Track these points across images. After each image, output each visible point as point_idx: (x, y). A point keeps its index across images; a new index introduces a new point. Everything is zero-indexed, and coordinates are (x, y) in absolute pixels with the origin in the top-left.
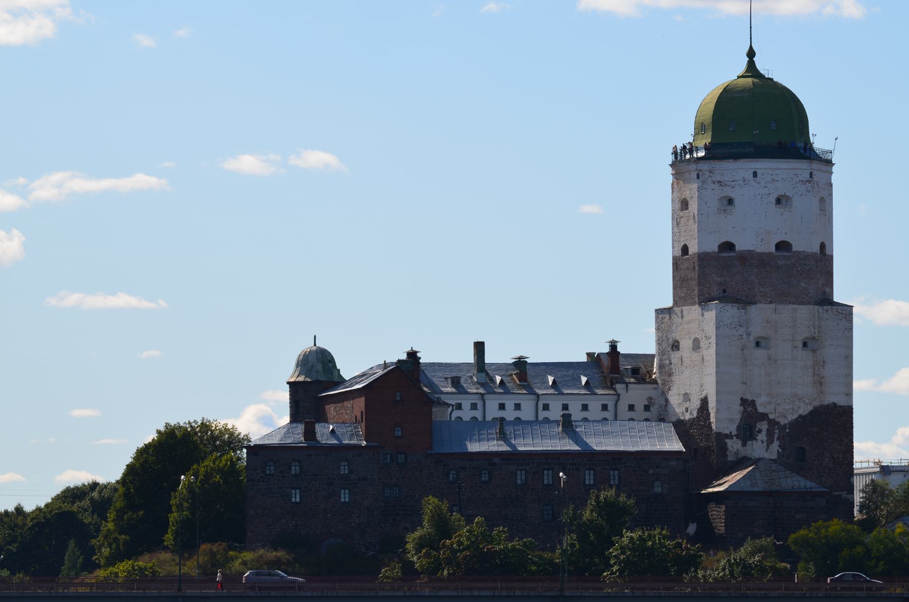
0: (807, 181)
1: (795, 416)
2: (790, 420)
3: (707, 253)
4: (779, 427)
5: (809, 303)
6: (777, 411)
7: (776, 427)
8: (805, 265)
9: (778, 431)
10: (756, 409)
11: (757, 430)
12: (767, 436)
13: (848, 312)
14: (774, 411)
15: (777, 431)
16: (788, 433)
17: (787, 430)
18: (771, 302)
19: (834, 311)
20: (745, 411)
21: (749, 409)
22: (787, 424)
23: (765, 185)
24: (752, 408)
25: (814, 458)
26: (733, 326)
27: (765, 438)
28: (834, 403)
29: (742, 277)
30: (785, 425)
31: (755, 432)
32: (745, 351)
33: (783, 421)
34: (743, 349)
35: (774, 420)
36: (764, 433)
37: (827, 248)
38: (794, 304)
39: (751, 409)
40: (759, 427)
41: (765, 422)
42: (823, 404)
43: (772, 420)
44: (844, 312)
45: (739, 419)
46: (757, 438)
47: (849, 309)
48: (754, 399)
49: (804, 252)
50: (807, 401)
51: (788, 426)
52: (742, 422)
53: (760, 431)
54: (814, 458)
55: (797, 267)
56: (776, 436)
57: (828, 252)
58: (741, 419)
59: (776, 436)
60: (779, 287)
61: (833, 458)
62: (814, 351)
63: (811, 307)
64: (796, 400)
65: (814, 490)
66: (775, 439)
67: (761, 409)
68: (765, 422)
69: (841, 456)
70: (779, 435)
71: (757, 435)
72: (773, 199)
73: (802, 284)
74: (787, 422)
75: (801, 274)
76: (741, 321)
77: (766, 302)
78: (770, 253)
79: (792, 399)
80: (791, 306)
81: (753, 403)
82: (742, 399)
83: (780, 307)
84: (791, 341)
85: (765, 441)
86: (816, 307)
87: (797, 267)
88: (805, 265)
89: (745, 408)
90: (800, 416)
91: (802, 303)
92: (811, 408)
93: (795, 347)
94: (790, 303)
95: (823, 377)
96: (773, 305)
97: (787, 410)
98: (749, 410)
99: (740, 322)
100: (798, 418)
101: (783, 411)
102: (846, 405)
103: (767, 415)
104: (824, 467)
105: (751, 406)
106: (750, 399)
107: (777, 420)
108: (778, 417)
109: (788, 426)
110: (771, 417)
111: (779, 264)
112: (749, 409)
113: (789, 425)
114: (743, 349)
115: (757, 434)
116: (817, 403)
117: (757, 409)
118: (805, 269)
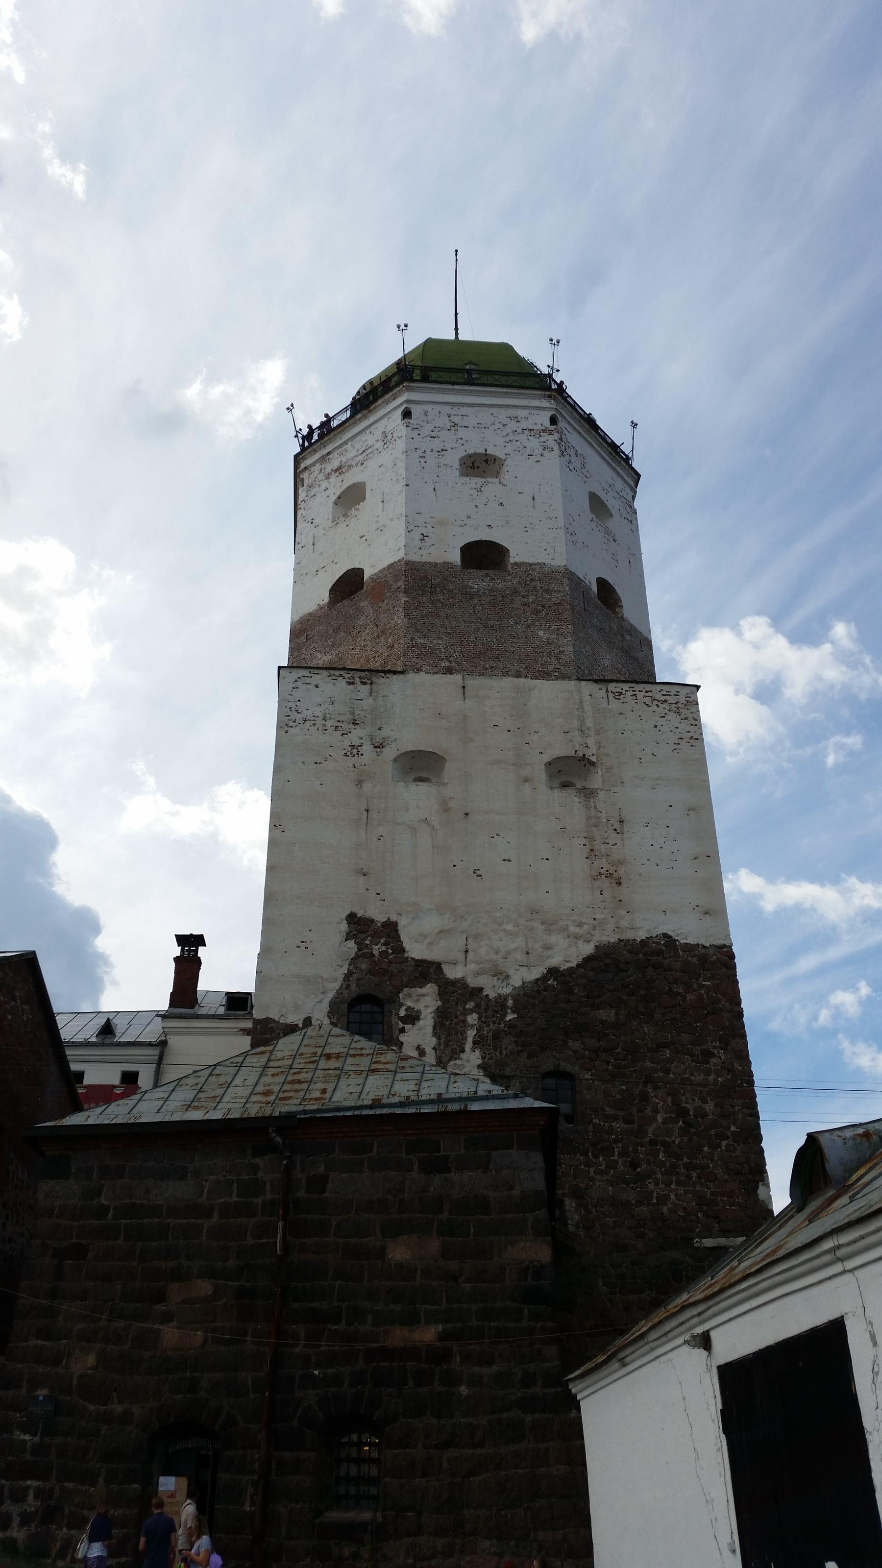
0: (544, 431)
1: (536, 974)
2: (518, 984)
3: (310, 614)
4: (478, 1006)
5: (563, 677)
6: (470, 955)
7: (470, 1005)
8: (547, 591)
9: (475, 1016)
10: (400, 949)
11: (402, 1013)
12: (435, 1034)
13: (682, 699)
14: (461, 956)
15: (472, 1019)
16: (511, 1025)
17: (510, 1017)
18: (449, 671)
19: (640, 695)
20: (363, 954)
21: (376, 949)
22: (509, 995)
23: (433, 434)
24: (385, 944)
25: (609, 1111)
26: (329, 723)
27: (429, 1041)
28: (665, 935)
29: (376, 628)
30: (501, 1001)
31: (394, 1020)
32: (367, 787)
33: (492, 988)
34: (359, 783)
35: (460, 983)
36: (427, 1022)
37: (624, 603)
38: (518, 676)
39: (384, 948)
40: (409, 1003)
41: (431, 989)
42: (629, 935)
43: (454, 983)
44: (670, 699)
45: (341, 978)
46: (403, 1038)
47: (684, 691)
48: (394, 918)
49: (542, 565)
50: (573, 929)
51: (510, 1002)
52: (348, 987)
53: (413, 1017)
54: (609, 1111)
55: (523, 596)
56: (471, 1034)
57: (628, 612)
58: (347, 977)
59: (471, 1034)
60: (472, 639)
61: (682, 1113)
62: (588, 794)
63: (571, 685)
64: (537, 924)
65: (475, 1107)
66: (469, 1045)
67: (416, 950)
68: (431, 989)
69: (710, 1107)
70: (478, 1030)
71: (402, 1030)
72: (454, 458)
73: (541, 633)
74: (508, 990)
75: (536, 612)
76: (357, 712)
77: (436, 670)
78: (447, 566)
79: (522, 921)
80: (508, 682)
81: (390, 930)
82: (352, 918)
83: (474, 683)
84: (514, 764)
85: (429, 1050)
86: (587, 688)
87: (523, 596)
88: (547, 591)
89: (360, 946)
90: (553, 972)
91: (544, 675)
92: (588, 949)
93: (526, 780)
94: (506, 673)
95: (621, 862)
96: (457, 678)
97: (508, 953)
98: (376, 953)
99: (353, 713)
100: (544, 979)
101: (494, 957)
102: (707, 945)
103: (437, 966)
104: (653, 1142)
105: (383, 940)
106: (380, 918)
107: (473, 982)
108: (477, 974)
109: (510, 1002)
110: (452, 973)
111: (471, 588)
112: (376, 949)
113: (515, 1000)
114: (359, 783)
115: (401, 1025)
116: (609, 937)
117: (403, 950)
118: (549, 600)
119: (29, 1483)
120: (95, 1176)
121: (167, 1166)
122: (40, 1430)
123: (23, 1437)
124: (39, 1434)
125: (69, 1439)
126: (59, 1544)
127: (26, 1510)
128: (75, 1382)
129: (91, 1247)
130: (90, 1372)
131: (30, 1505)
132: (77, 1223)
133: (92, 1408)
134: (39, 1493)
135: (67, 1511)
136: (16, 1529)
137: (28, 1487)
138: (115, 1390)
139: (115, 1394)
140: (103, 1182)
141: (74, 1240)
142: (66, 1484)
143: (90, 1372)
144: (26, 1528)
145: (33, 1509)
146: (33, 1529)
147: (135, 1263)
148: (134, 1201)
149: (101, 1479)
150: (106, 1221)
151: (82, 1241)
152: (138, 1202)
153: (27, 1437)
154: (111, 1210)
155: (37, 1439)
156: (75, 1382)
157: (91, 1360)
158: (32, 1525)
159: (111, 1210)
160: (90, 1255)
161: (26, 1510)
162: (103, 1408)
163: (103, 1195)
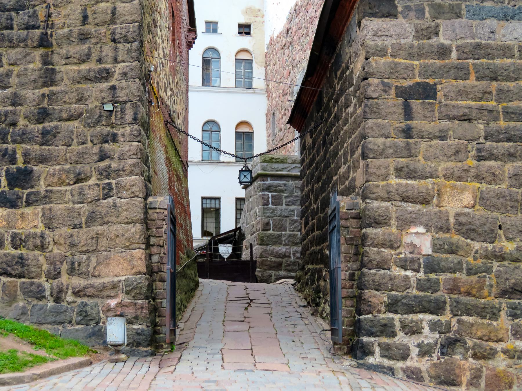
119: (421, 316)
120: (427, 15)
121: (509, 6)
122: (422, 266)
123: (403, 273)
124: (422, 270)
125: (457, 275)
126: (468, 374)
127: (423, 342)
128: (452, 220)
129: (439, 87)
130: (467, 210)
131: (426, 337)
132: (417, 63)
133: (477, 245)
134: (434, 326)
135: (470, 343)
136: (416, 359)
137: (422, 321)
138: (500, 227)
139: (501, 232)
140: (437, 21)
141: (418, 79)
142: (465, 318)
143: (467, 210)
144: (427, 358)
145: (431, 341)
146: (435, 359)
147: (494, 103)
148: (477, 40)
149: (502, 313)
150: (450, 61)
151: (427, 81)
152: (484, 42)
153: (409, 273)
154: (454, 49)
155: (421, 275)
156: (452, 220)
157: (468, 198)
158: (433, 355)
159: (454, 49)
160: (440, 95)
161: (423, 342)
162: (490, 247)
163: (441, 33)
